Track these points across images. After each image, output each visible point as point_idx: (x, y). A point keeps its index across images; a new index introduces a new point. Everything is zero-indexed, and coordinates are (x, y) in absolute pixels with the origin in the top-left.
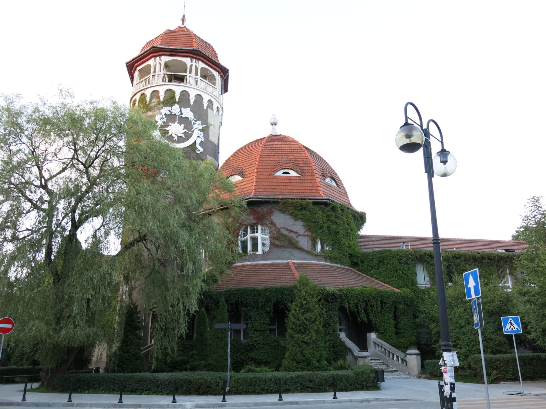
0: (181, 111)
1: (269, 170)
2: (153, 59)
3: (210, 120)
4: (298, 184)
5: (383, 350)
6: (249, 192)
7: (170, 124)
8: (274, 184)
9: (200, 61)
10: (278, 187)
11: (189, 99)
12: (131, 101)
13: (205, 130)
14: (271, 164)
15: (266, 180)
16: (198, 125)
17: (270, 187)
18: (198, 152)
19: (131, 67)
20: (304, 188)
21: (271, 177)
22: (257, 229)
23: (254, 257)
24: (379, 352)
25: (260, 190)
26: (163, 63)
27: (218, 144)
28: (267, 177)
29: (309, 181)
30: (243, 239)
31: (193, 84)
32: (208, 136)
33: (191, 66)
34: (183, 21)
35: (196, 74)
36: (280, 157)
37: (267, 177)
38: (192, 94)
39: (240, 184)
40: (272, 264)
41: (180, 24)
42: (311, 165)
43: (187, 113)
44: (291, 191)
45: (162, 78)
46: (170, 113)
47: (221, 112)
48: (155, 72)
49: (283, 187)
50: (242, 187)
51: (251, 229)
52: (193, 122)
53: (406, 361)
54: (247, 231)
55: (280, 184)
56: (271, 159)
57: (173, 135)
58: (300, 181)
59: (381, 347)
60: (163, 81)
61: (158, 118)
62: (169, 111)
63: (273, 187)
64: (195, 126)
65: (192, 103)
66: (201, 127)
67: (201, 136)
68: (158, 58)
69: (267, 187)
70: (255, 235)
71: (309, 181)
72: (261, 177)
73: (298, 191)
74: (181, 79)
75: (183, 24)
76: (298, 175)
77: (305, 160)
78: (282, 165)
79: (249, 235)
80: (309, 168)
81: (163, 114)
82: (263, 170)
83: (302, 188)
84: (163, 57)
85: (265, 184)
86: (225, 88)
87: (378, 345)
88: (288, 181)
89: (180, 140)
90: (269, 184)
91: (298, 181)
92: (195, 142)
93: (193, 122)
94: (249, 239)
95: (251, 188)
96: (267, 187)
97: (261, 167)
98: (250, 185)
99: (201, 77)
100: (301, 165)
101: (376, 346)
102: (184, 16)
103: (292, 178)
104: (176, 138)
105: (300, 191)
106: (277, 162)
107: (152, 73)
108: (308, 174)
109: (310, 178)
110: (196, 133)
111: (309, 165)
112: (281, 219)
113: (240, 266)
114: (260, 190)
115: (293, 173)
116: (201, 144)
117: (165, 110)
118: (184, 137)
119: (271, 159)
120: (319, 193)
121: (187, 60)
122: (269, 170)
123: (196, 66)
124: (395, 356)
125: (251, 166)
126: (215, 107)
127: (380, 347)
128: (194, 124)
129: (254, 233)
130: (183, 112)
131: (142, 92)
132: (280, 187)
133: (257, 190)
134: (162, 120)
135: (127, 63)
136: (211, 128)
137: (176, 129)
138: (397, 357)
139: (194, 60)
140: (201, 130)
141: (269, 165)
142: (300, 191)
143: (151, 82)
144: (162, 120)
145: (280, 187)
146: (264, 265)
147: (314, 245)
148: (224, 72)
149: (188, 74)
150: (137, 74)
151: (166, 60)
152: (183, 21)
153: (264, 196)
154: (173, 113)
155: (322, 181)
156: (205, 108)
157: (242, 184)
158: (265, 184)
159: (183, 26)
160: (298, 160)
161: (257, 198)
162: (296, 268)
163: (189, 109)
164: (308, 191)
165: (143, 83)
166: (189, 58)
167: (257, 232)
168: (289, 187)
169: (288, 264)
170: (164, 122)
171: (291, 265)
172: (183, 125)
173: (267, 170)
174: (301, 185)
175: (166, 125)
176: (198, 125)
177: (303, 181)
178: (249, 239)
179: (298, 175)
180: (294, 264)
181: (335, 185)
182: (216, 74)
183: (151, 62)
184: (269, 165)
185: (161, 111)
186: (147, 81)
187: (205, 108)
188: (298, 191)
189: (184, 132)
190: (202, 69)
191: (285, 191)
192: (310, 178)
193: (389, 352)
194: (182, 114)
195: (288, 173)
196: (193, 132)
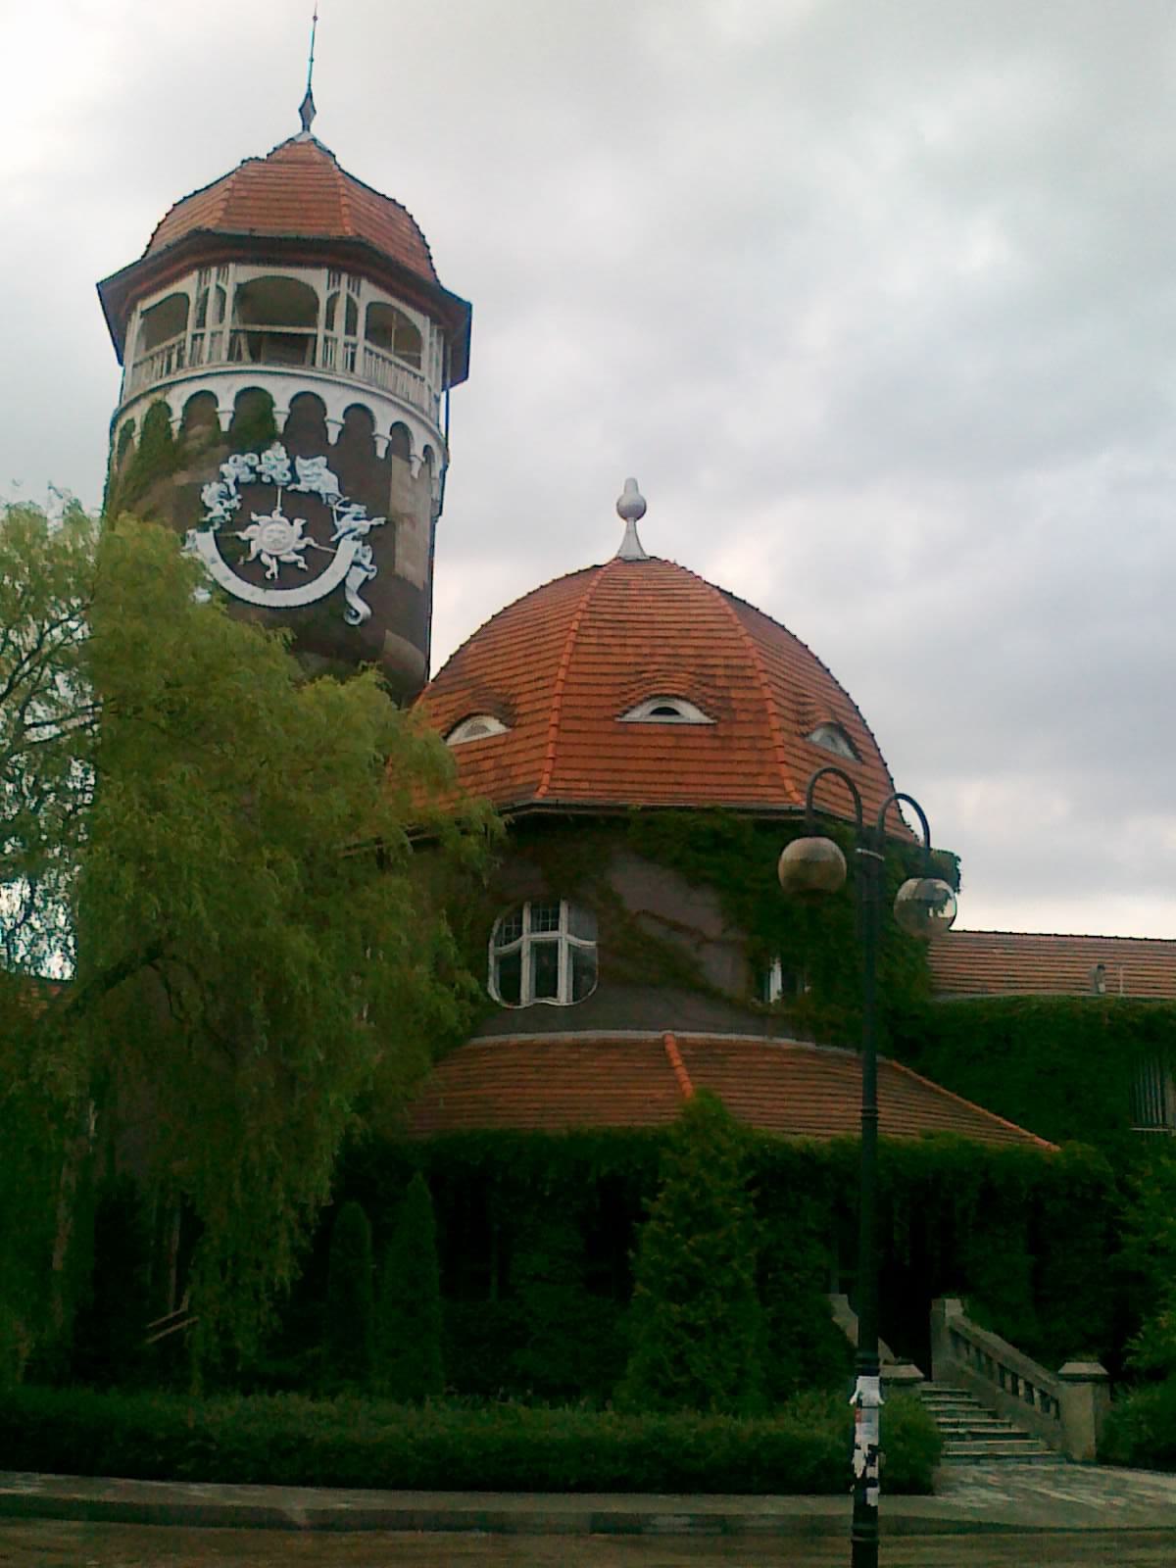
0: (292, 469)
1: (603, 702)
2: (196, 274)
3: (401, 499)
4: (707, 755)
5: (984, 1360)
6: (529, 778)
7: (254, 517)
8: (620, 752)
9: (364, 283)
10: (633, 765)
11: (324, 423)
12: (114, 424)
13: (379, 540)
16: (353, 521)
18: (353, 622)
19: (118, 296)
20: (727, 768)
21: (609, 726)
22: (557, 915)
23: (542, 1018)
24: (967, 1368)
25: (569, 775)
26: (230, 291)
28: (595, 726)
29: (746, 744)
30: (506, 949)
31: (339, 367)
32: (392, 555)
33: (332, 301)
34: (307, 111)
35: (350, 329)
36: (646, 651)
37: (595, 726)
38: (336, 404)
39: (500, 750)
40: (605, 1046)
41: (294, 127)
42: (756, 684)
43: (318, 476)
44: (680, 779)
45: (226, 345)
47: (438, 466)
48: (201, 323)
50: (506, 761)
51: (534, 915)
52: (336, 507)
53: (1057, 1402)
54: (520, 921)
55: (641, 753)
57: (264, 558)
58: (717, 743)
59: (978, 1350)
60: (230, 358)
61: (210, 493)
62: (252, 469)
64: (344, 525)
65: (333, 438)
66: (364, 527)
67: (366, 562)
68: (214, 270)
70: (549, 935)
71: (746, 744)
73: (707, 779)
74: (295, 349)
75: (306, 127)
76: (705, 719)
77: (735, 662)
78: (650, 682)
79: (527, 939)
80: (751, 695)
81: (230, 481)
82: (581, 701)
83: (720, 768)
84: (232, 266)
85: (587, 751)
86: (457, 368)
87: (967, 1343)
88: (670, 742)
89: (290, 576)
91: (707, 743)
92: (343, 583)
93: (336, 507)
94: (526, 950)
95: (536, 766)
97: (575, 689)
98: (535, 754)
99: (369, 334)
100: (720, 682)
101: (962, 1346)
102: (309, 95)
103: (687, 730)
104: (275, 569)
106: (632, 669)
107: (191, 328)
108: (743, 717)
110: (347, 550)
111: (748, 683)
112: (641, 886)
113: (492, 1049)
114: (569, 775)
115: (690, 713)
116: (364, 590)
117: (235, 468)
118: (302, 565)
119: (613, 659)
120: (782, 787)
121: (317, 280)
122: (603, 702)
123: (349, 299)
124: (1021, 1383)
125: (541, 683)
126: (417, 450)
127: (972, 1351)
128: (341, 515)
130: (300, 472)
131: (158, 396)
133: (559, 774)
134: (227, 504)
136: (404, 528)
137: (274, 535)
138: (1029, 1386)
140: (364, 539)
143: (186, 361)
144: (227, 504)
146: (577, 1046)
147: (761, 981)
148: (454, 318)
149: (321, 331)
150: (136, 323)
151: (243, 280)
152: (307, 111)
153: (585, 791)
154: (265, 479)
155: (798, 741)
156: (381, 453)
157: (507, 749)
158: (587, 751)
159: (304, 138)
161: (557, 806)
162: (687, 1060)
163: (322, 460)
164: (741, 780)
165: (157, 365)
166: (325, 272)
167: (555, 928)
168: (673, 766)
169: (661, 1045)
170: (232, 511)
171: (671, 1048)
172: (299, 523)
173: (596, 701)
175: (239, 519)
178: (526, 950)
179: (705, 719)
180: (682, 1043)
181: (849, 754)
182: (421, 322)
183: (188, 285)
185: (224, 468)
186: (175, 358)
187: (381, 453)
188: (707, 779)
189: (301, 545)
190: (371, 306)
191: (657, 778)
193: (1001, 1367)
194: (296, 479)
195: (674, 712)
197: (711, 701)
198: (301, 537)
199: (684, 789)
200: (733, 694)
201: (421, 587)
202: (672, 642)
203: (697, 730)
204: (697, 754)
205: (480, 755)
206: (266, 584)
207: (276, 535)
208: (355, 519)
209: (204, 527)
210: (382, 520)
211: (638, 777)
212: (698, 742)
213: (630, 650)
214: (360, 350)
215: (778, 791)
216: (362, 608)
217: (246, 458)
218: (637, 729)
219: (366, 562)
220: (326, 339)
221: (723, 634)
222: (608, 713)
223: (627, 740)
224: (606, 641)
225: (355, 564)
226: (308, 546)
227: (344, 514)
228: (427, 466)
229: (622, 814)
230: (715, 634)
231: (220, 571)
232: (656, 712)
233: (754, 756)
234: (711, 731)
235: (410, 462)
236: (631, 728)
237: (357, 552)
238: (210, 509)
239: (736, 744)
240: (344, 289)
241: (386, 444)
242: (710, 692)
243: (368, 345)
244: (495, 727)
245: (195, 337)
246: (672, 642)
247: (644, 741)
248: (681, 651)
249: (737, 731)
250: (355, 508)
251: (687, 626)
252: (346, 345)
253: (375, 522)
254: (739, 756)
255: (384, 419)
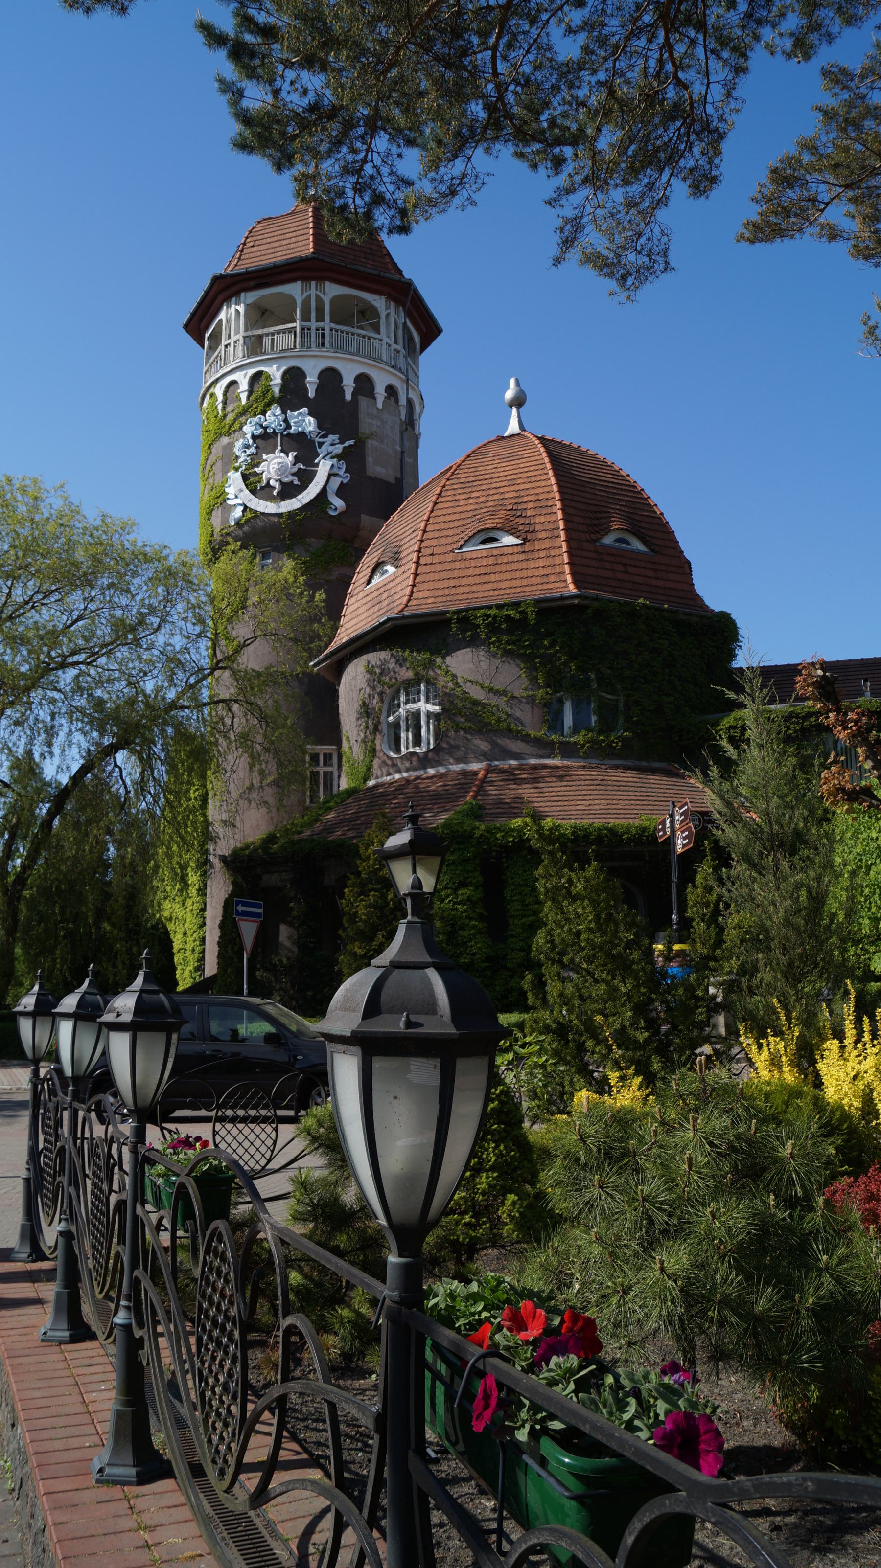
0: (286, 421)
4: (515, 566)
7: (265, 457)
8: (456, 574)
9: (327, 283)
14: (456, 524)
15: (438, 567)
17: (446, 584)
20: (529, 573)
21: (450, 557)
22: (419, 692)
27: (400, 482)
28: (442, 558)
31: (313, 345)
32: (363, 466)
35: (320, 318)
36: (482, 499)
37: (442, 558)
39: (391, 585)
42: (554, 509)
44: (495, 586)
46: (260, 430)
48: (229, 337)
49: (477, 580)
50: (393, 591)
55: (470, 572)
56: (459, 509)
57: (272, 483)
58: (522, 557)
63: (452, 583)
64: (322, 451)
65: (311, 394)
66: (338, 449)
67: (341, 472)
68: (234, 299)
69: (441, 584)
71: (542, 554)
72: (429, 560)
73: (514, 583)
80: (548, 518)
81: (249, 436)
83: (524, 574)
84: (243, 294)
85: (437, 576)
88: (491, 561)
89: (288, 491)
90: (446, 575)
91: (516, 558)
92: (324, 492)
93: (317, 439)
96: (441, 584)
105: (519, 583)
106: (471, 514)
107: (224, 343)
108: (544, 535)
109: (547, 544)
116: (341, 492)
118: (296, 482)
119: (459, 509)
121: (295, 290)
122: (450, 540)
123: (318, 298)
128: (321, 444)
129: (414, 702)
131: (211, 391)
132: (471, 580)
134: (248, 452)
135: (187, 327)
136: (371, 443)
139: (313, 283)
140: (339, 457)
141: (452, 525)
142: (519, 583)
145: (471, 580)
156: (348, 397)
158: (437, 576)
160: (525, 499)
163: (304, 410)
164: (539, 580)
166: (299, 283)
167: (419, 700)
168: (493, 578)
174: (524, 565)
175: (255, 460)
176: (332, 445)
177: (530, 556)
182: (379, 302)
183: (222, 316)
184: (452, 525)
187: (348, 397)
188: (514, 583)
189: (295, 469)
190: (335, 300)
191: (480, 588)
192: (547, 544)
194: (288, 426)
196: (317, 465)
197: (521, 528)
198: (295, 464)
199: (497, 593)
200: (537, 520)
201: (393, 481)
202: (502, 490)
203: (510, 550)
204: (509, 567)
205: (382, 590)
206: (270, 498)
207: (276, 466)
208: (332, 445)
209: (237, 469)
210: (352, 442)
211: (467, 589)
212: (510, 558)
213: (471, 501)
214: (327, 332)
215: (563, 584)
216: (338, 503)
217: (256, 419)
218: (468, 556)
219: (341, 472)
220: (303, 329)
221: (538, 478)
222: (449, 548)
223: (463, 564)
224: (457, 497)
225: (330, 475)
226: (300, 469)
227: (323, 443)
228: (392, 399)
229: (442, 617)
230: (533, 479)
231: (246, 496)
232: (484, 542)
233: (548, 562)
234: (519, 549)
235: (374, 398)
236: (465, 556)
237: (333, 466)
238: (237, 457)
239: (536, 555)
240: (313, 292)
241: (352, 390)
242: (521, 521)
243: (333, 325)
244: (390, 569)
245: (226, 346)
246: (502, 490)
247: (473, 563)
248: (506, 496)
249: (537, 545)
250: (331, 437)
251: (513, 477)
252: (317, 330)
253: (347, 444)
254: (541, 563)
255: (349, 374)
